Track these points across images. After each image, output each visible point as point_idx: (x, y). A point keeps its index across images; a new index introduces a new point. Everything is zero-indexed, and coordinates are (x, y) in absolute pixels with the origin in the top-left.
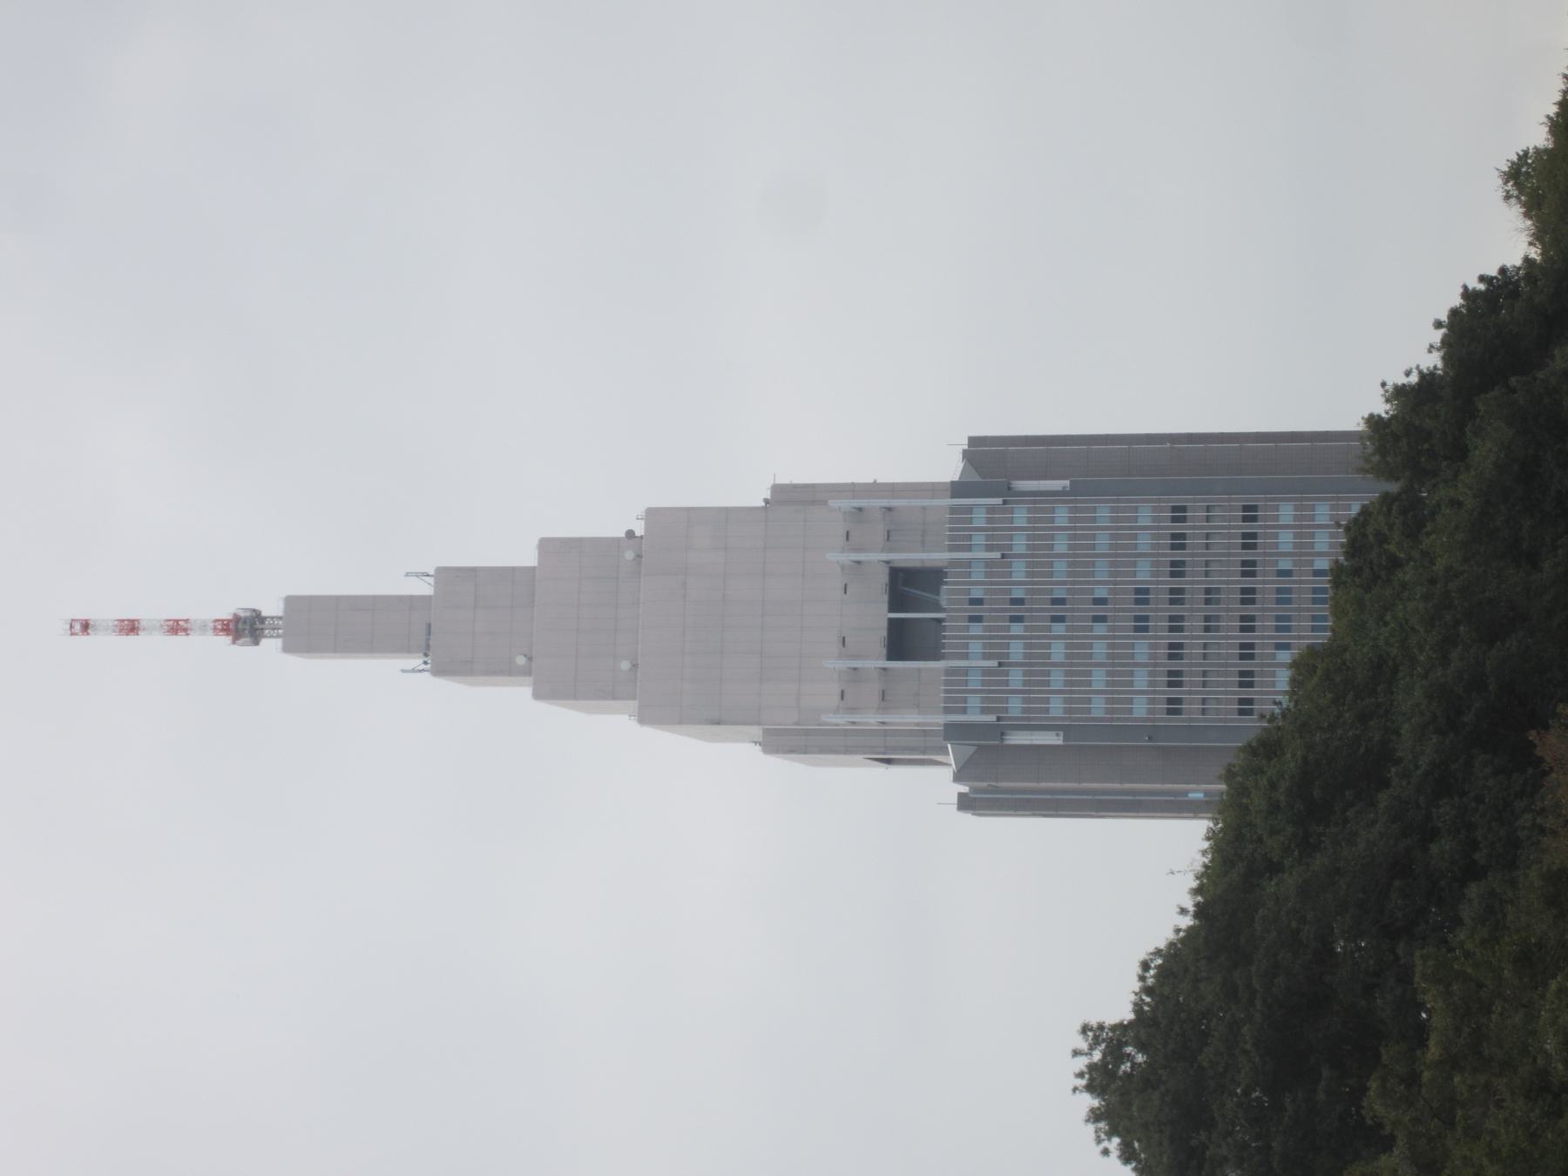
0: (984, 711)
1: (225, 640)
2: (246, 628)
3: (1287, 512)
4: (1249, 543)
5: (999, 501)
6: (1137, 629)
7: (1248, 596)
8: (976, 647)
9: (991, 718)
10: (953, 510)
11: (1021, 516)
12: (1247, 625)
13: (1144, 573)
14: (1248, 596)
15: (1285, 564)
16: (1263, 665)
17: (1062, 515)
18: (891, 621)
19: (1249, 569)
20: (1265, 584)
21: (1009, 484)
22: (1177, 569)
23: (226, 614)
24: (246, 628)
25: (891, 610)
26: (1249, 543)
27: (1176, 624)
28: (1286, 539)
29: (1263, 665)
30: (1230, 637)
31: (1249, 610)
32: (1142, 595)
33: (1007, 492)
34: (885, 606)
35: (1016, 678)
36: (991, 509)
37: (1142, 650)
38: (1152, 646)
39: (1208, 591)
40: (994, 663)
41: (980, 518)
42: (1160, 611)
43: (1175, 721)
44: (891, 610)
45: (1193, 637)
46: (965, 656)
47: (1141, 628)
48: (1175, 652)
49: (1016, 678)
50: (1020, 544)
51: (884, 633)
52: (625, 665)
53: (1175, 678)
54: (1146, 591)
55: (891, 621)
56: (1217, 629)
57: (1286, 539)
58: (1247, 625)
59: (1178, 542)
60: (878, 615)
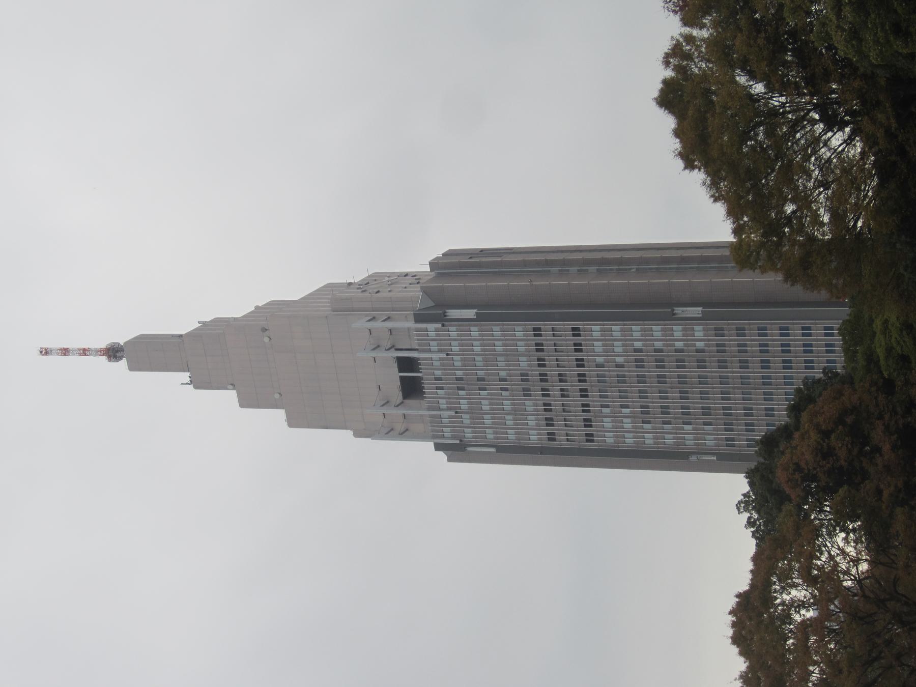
0: (454, 437)
1: (104, 359)
2: (113, 353)
3: (596, 330)
4: (578, 347)
5: (439, 325)
6: (525, 395)
7: (582, 378)
8: (443, 403)
9: (458, 442)
10: (418, 330)
11: (453, 331)
12: (584, 393)
13: (524, 364)
14: (582, 378)
15: (600, 360)
16: (596, 416)
17: (475, 333)
18: (401, 377)
19: (580, 363)
20: (590, 371)
21: (445, 313)
22: (541, 363)
23: (103, 345)
24: (113, 353)
25: (400, 371)
26: (578, 347)
27: (545, 393)
28: (598, 347)
29: (596, 416)
30: (575, 402)
31: (583, 385)
32: (524, 377)
33: (442, 319)
34: (397, 371)
35: (466, 419)
37: (529, 405)
38: (536, 405)
39: (560, 375)
40: (453, 413)
41: (432, 334)
42: (536, 387)
43: (552, 444)
44: (400, 371)
46: (439, 409)
47: (527, 393)
48: (547, 407)
49: (466, 419)
50: (456, 349)
51: (399, 384)
52: (277, 396)
53: (549, 422)
54: (527, 375)
55: (401, 377)
56: (568, 396)
57: (598, 347)
58: (584, 393)
59: (539, 347)
60: (394, 375)
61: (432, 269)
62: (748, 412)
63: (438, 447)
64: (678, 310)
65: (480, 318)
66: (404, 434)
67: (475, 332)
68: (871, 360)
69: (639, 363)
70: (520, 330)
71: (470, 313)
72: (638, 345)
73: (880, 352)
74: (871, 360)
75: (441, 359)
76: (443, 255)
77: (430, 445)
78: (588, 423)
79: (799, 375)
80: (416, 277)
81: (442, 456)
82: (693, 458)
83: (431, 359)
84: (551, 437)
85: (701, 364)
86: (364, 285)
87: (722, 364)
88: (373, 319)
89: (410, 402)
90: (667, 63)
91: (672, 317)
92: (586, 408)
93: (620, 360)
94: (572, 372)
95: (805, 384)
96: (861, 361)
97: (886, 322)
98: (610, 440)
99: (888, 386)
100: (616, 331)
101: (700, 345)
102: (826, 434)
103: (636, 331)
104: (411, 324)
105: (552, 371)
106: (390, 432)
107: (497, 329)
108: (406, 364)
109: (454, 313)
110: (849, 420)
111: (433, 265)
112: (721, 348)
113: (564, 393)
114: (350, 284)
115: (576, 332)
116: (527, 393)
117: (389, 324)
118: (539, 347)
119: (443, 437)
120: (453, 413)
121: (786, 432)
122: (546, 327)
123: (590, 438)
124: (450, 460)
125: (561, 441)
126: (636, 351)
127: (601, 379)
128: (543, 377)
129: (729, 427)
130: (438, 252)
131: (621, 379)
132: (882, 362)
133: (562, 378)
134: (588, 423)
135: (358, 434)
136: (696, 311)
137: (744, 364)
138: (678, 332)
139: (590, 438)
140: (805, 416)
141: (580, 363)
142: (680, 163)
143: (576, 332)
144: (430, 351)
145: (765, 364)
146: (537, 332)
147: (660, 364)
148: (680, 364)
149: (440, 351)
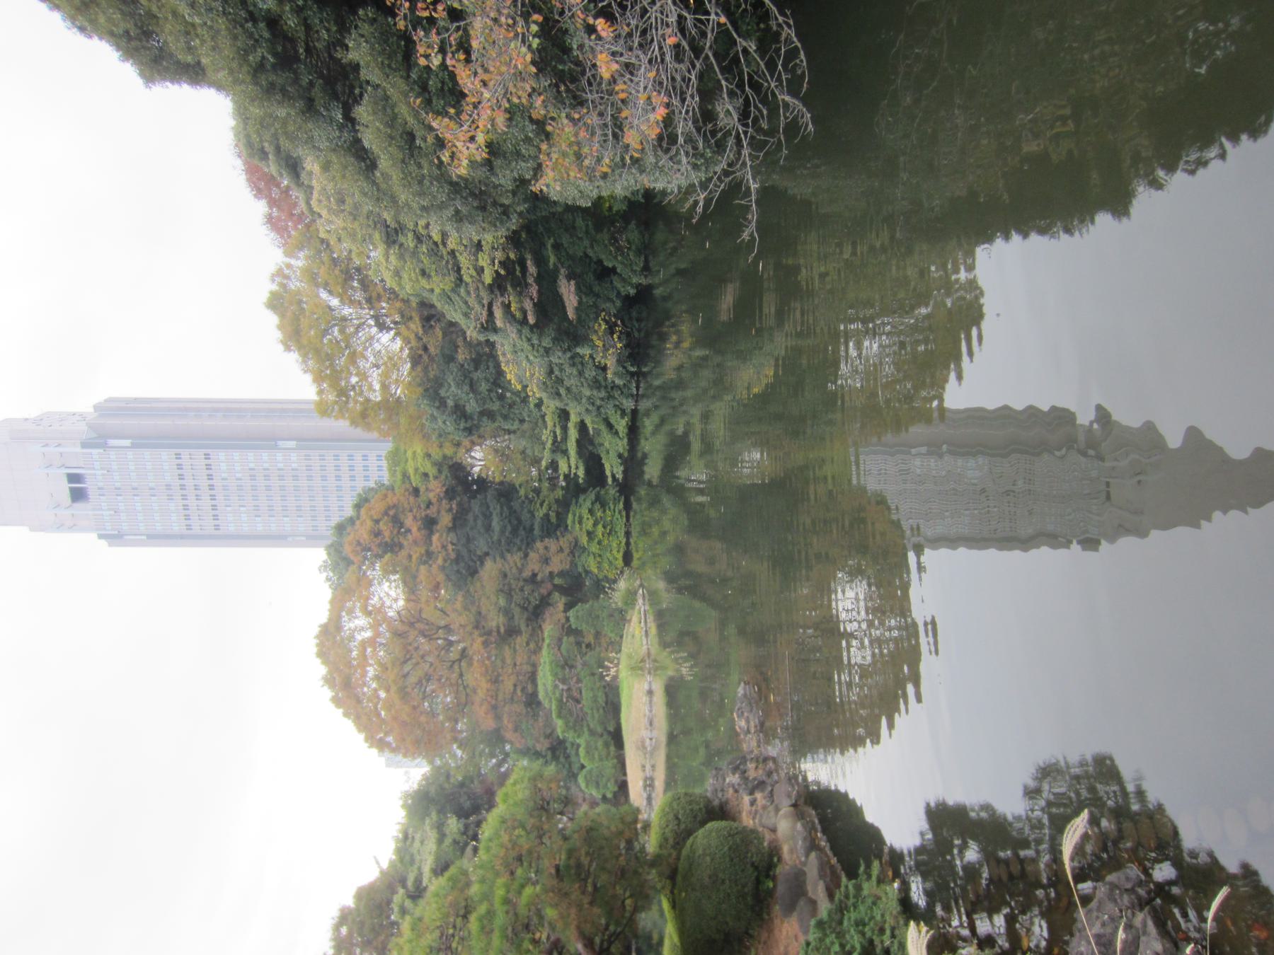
3: (222, 455)
4: (208, 467)
5: (101, 451)
7: (211, 487)
11: (113, 455)
12: (213, 497)
14: (211, 487)
15: (224, 475)
19: (210, 477)
22: (181, 477)
26: (208, 467)
27: (184, 497)
28: (224, 467)
32: (168, 487)
33: (104, 446)
36: (99, 454)
45: (192, 502)
47: (170, 498)
48: (186, 507)
50: (115, 467)
53: (187, 517)
57: (224, 467)
58: (213, 497)
59: (180, 467)
60: (65, 487)
61: (96, 411)
62: (327, 508)
63: (101, 537)
64: (281, 443)
65: (134, 446)
66: (73, 528)
67: (130, 455)
68: (405, 476)
69: (253, 477)
70: (166, 455)
71: (127, 442)
72: (252, 465)
73: (411, 471)
74: (405, 476)
75: (103, 475)
76: (106, 401)
77: (94, 535)
78: (216, 517)
79: (360, 485)
80: (83, 416)
81: (103, 542)
82: (290, 539)
83: (95, 475)
84: (189, 527)
85: (296, 478)
86: (38, 421)
87: (310, 478)
88: (47, 445)
89: (76, 505)
90: (273, 281)
91: (276, 447)
92: (214, 507)
93: (239, 475)
94: (204, 483)
95: (363, 490)
96: (399, 476)
97: (414, 453)
98: (232, 528)
99: (416, 491)
100: (236, 455)
101: (294, 465)
102: (377, 522)
103: (251, 455)
104: (79, 450)
105: (189, 482)
106: (60, 527)
107: (147, 454)
108: (74, 478)
109: (113, 442)
110: (391, 513)
111: (97, 408)
112: (309, 468)
113: (198, 497)
114: (26, 419)
115: (207, 456)
116: (170, 498)
117: (60, 449)
118: (180, 467)
119: (105, 529)
120: (112, 512)
121: (351, 521)
122: (185, 454)
123: (217, 527)
124: (110, 545)
125: (196, 529)
126: (250, 469)
127: (225, 488)
128: (183, 487)
129: (314, 518)
130: (99, 397)
131: (240, 488)
132: (412, 477)
133: (196, 488)
134: (216, 517)
135: (32, 529)
136: (292, 444)
137: (324, 478)
138: (279, 456)
139: (217, 527)
140: (363, 511)
141: (210, 477)
142: (281, 347)
143: (207, 456)
144: (94, 469)
145: (338, 478)
146: (178, 456)
147: (267, 477)
148: (281, 478)
149: (102, 469)
